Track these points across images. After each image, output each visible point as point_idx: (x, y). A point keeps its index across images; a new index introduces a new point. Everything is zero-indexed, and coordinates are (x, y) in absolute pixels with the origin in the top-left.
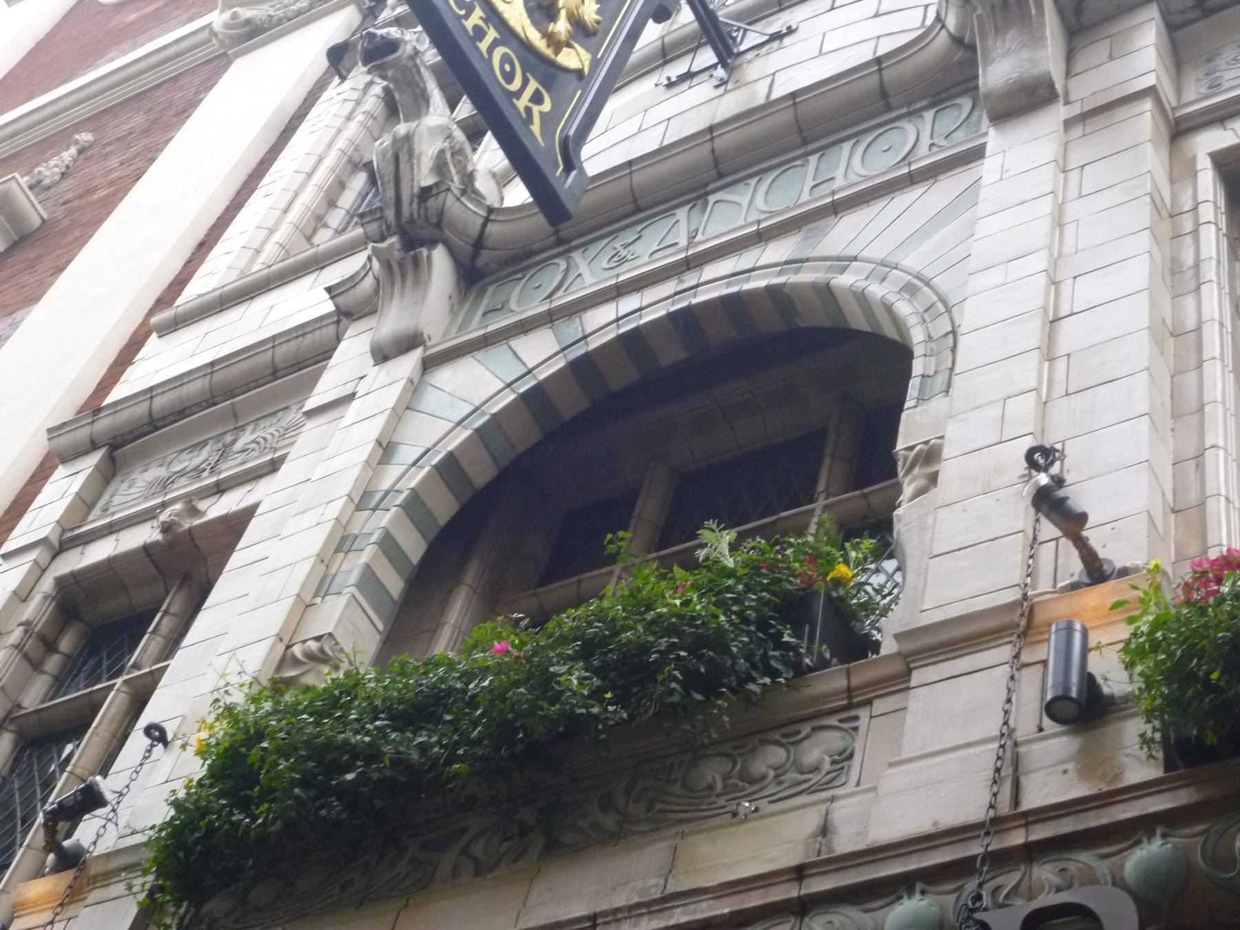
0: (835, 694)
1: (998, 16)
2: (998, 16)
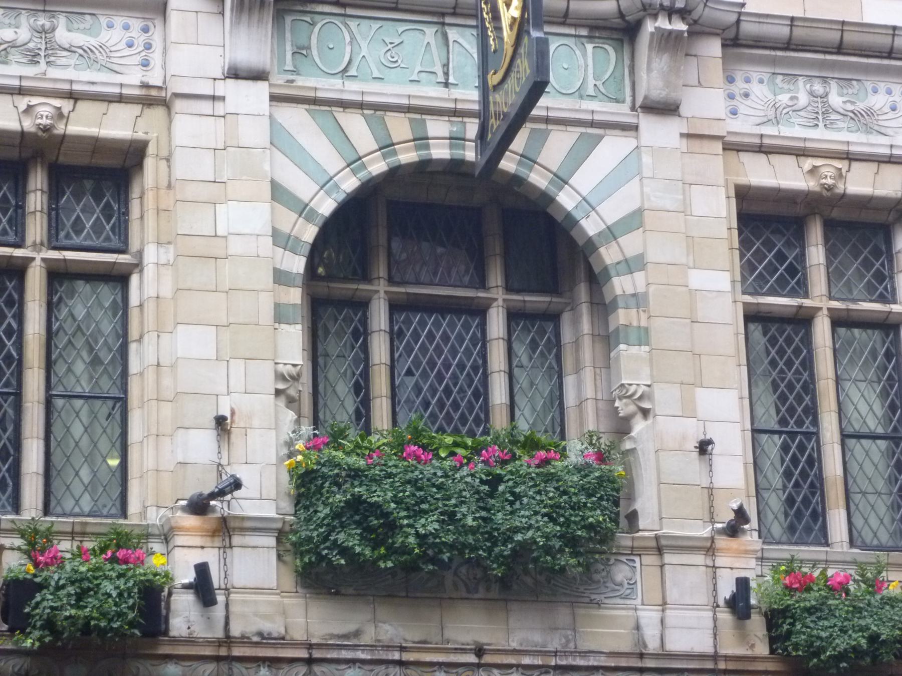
0: (625, 547)
1: (663, 42)
2: (663, 42)
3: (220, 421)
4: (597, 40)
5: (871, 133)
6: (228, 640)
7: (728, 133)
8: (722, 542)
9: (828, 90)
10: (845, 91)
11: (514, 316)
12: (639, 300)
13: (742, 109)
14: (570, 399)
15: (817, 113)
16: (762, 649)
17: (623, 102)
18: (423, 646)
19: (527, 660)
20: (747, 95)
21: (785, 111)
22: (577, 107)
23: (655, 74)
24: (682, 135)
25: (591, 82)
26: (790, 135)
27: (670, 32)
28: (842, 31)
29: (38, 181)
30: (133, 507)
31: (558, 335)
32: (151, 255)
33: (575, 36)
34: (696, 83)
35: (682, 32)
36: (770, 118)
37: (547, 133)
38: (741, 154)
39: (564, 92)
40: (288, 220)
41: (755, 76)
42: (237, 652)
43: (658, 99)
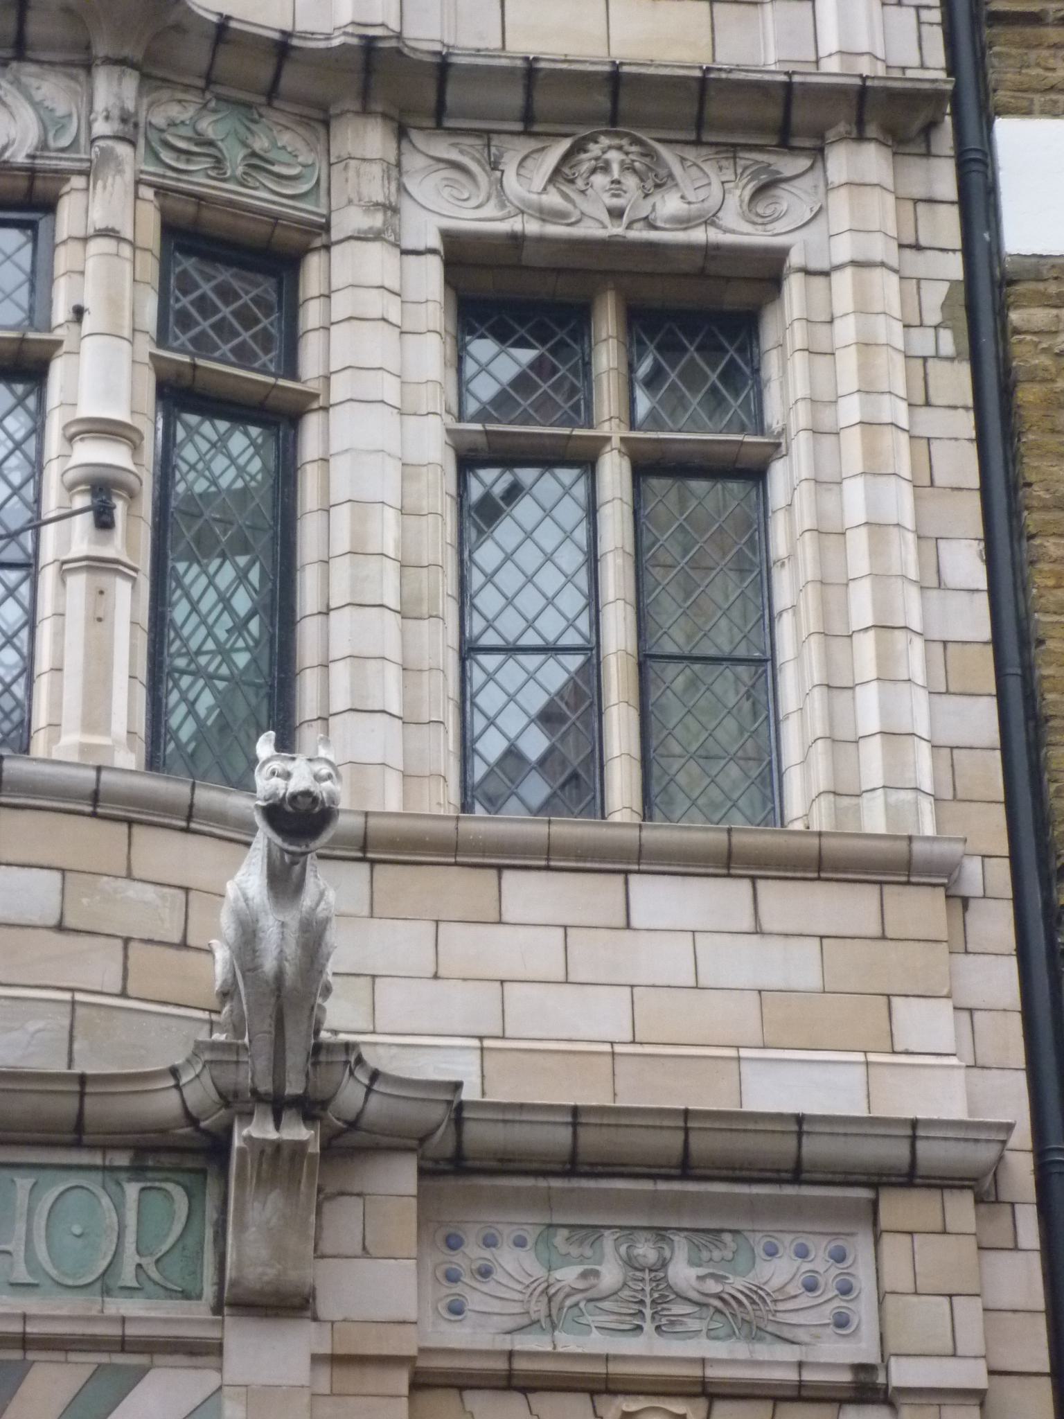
2: (265, 1166)
4: (150, 1175)
5: (761, 1340)
7: (422, 1350)
9: (667, 1253)
10: (705, 1255)
13: (475, 1302)
15: (642, 1302)
17: (199, 1297)
20: (485, 1273)
21: (568, 1302)
22: (94, 1312)
23: (252, 1234)
24: (316, 1359)
25: (130, 1258)
26: (579, 1350)
27: (278, 1146)
28: (686, 1130)
33: (104, 1169)
34: (358, 1250)
35: (299, 1148)
36: (534, 1317)
37: (26, 1367)
38: (468, 1395)
39: (70, 1282)
41: (507, 1233)
43: (258, 1287)
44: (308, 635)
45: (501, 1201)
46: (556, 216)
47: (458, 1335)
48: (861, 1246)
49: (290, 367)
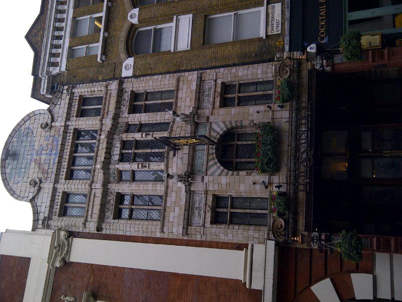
3: (254, 184)
6: (287, 183)
8: (272, 109)
11: (238, 140)
12: (236, 122)
14: (250, 132)
16: (289, 103)
18: (288, 154)
19: (290, 139)
29: (218, 210)
30: (266, 197)
31: (240, 134)
32: (229, 194)
40: (224, 173)
42: (289, 182)
44: (158, 122)
45: (201, 104)
46: (127, 107)
47: (210, 108)
48: (205, 82)
49: (137, 125)
